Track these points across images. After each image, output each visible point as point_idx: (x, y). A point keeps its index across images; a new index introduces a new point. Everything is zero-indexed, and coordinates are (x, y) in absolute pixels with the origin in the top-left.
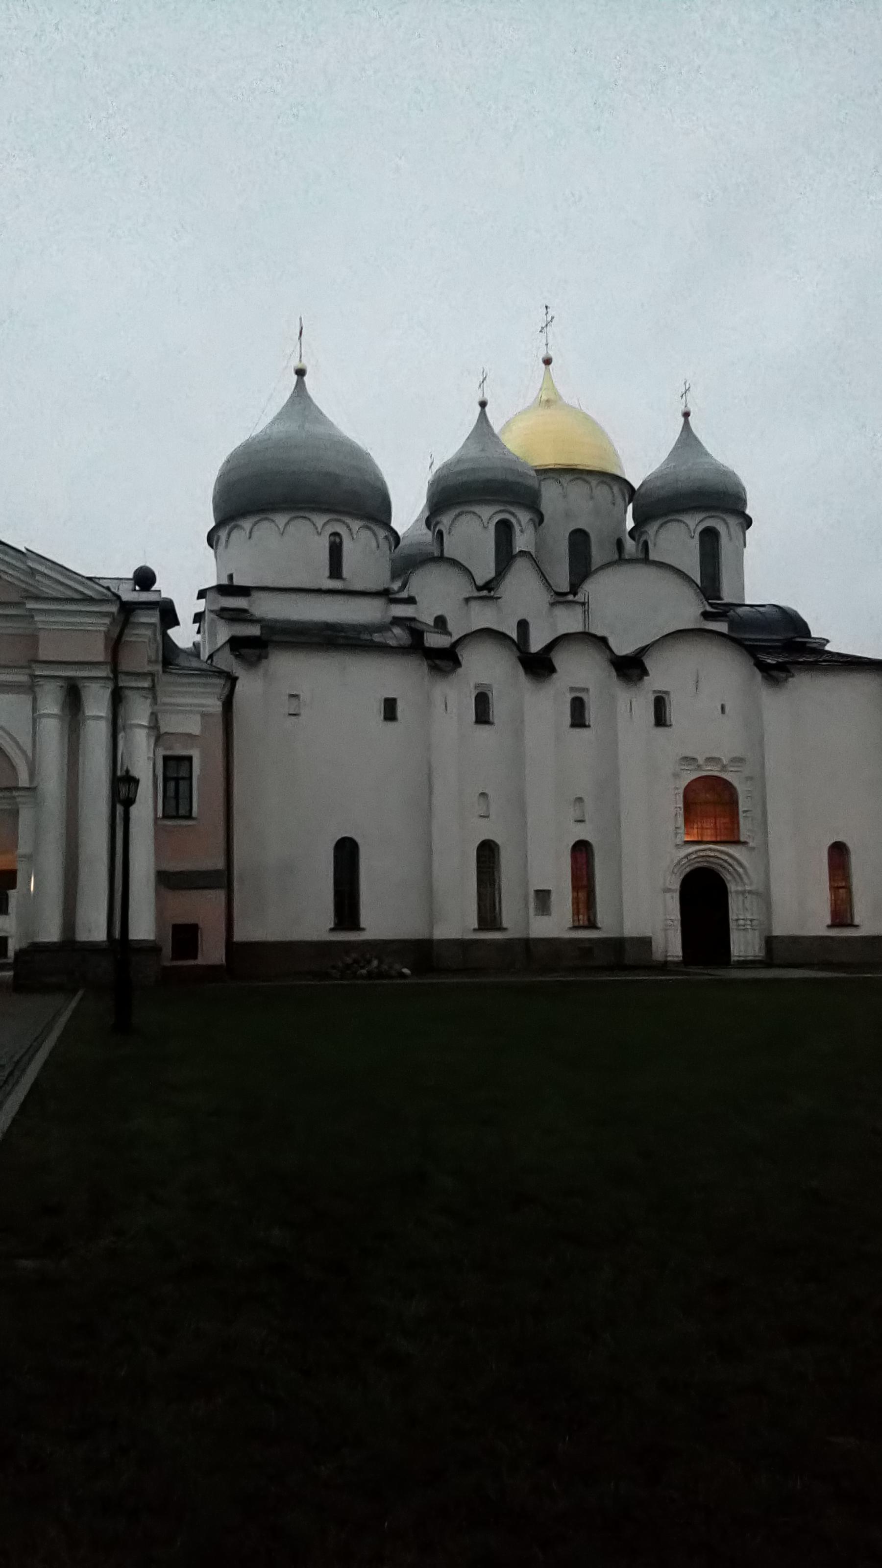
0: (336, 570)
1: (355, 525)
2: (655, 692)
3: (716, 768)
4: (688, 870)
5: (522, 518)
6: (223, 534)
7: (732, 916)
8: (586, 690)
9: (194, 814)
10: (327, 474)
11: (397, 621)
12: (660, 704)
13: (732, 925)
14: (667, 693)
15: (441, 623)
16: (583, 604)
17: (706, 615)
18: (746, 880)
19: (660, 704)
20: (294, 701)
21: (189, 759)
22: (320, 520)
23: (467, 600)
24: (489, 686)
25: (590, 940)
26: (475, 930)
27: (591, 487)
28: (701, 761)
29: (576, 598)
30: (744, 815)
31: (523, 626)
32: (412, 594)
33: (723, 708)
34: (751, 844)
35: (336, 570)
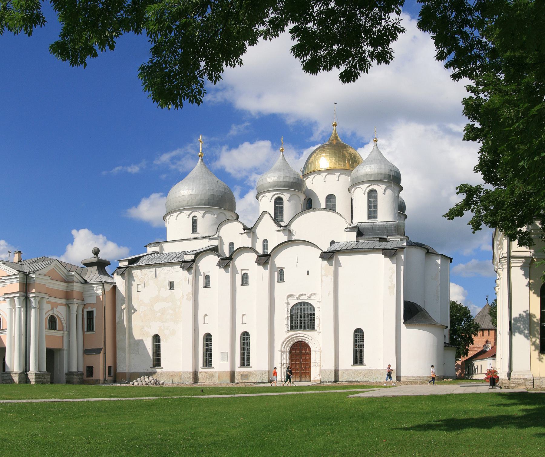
7: (312, 361)
13: (312, 365)
19: (281, 272)
30: (317, 318)
34: (317, 331)
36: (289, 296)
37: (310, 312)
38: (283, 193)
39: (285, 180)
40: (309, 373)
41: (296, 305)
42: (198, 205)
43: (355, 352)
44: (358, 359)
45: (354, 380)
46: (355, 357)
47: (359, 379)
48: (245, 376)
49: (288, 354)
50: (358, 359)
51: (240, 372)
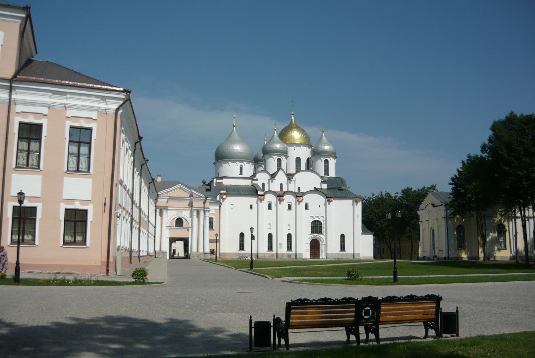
0: (241, 173)
1: (245, 163)
2: (305, 203)
3: (318, 218)
4: (311, 239)
5: (283, 159)
6: (217, 164)
7: (320, 249)
8: (291, 203)
9: (214, 228)
10: (239, 152)
11: (253, 185)
12: (306, 205)
13: (320, 251)
14: (308, 203)
15: (263, 184)
16: (294, 180)
17: (322, 182)
18: (323, 242)
19: (306, 205)
20: (232, 206)
21: (213, 218)
22: (238, 163)
23: (269, 179)
24: (271, 202)
25: (290, 253)
26: (267, 251)
27: (301, 147)
28: (314, 217)
29: (293, 179)
31: (281, 185)
32: (257, 178)
33: (319, 207)
34: (324, 234)
35: (241, 173)
36: (311, 217)
37: (320, 225)
38: (282, 157)
39: (283, 149)
40: (319, 255)
41: (313, 221)
42: (242, 159)
43: (341, 245)
44: (343, 248)
45: (341, 258)
46: (341, 247)
47: (343, 257)
48: (289, 256)
49: (309, 244)
50: (343, 248)
51: (287, 254)
